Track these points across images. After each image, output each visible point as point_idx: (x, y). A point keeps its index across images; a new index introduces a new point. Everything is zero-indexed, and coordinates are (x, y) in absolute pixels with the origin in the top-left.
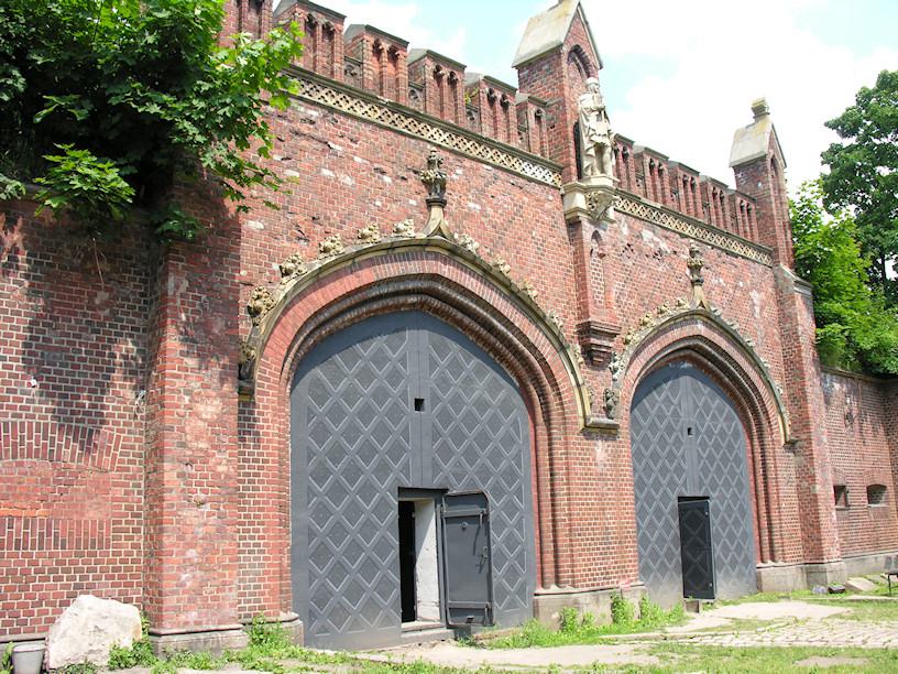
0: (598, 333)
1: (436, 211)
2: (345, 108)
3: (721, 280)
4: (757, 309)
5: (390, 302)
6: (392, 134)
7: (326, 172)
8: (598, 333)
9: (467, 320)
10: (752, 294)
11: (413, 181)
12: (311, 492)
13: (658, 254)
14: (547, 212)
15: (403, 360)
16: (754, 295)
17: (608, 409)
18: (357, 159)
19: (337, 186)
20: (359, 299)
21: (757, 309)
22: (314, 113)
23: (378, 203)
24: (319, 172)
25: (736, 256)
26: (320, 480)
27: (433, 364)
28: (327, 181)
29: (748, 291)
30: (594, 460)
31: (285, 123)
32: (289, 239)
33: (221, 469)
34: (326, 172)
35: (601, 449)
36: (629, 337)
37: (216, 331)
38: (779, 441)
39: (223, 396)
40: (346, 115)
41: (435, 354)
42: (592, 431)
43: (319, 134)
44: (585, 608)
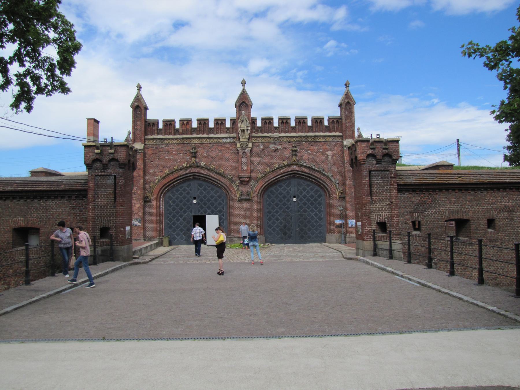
0: (242, 178)
1: (193, 158)
2: (171, 142)
3: (309, 152)
4: (330, 157)
5: (185, 179)
6: (183, 144)
7: (166, 157)
8: (242, 178)
9: (206, 179)
10: (327, 153)
11: (188, 153)
12: (168, 217)
13: (276, 150)
14: (231, 150)
15: (191, 190)
16: (330, 153)
17: (248, 195)
18: (174, 152)
19: (169, 159)
20: (175, 180)
21: (330, 157)
22: (164, 146)
23: (179, 160)
24: (165, 157)
25: (320, 142)
26: (170, 215)
27: (199, 190)
28: (167, 159)
29: (325, 152)
30: (243, 207)
31: (157, 150)
32: (158, 172)
33: (140, 215)
34: (167, 157)
35: (245, 205)
36: (258, 176)
37: (139, 193)
38: (337, 197)
39: (140, 203)
40: (171, 144)
41: (199, 187)
42: (241, 200)
43: (165, 150)
44: (235, 241)
